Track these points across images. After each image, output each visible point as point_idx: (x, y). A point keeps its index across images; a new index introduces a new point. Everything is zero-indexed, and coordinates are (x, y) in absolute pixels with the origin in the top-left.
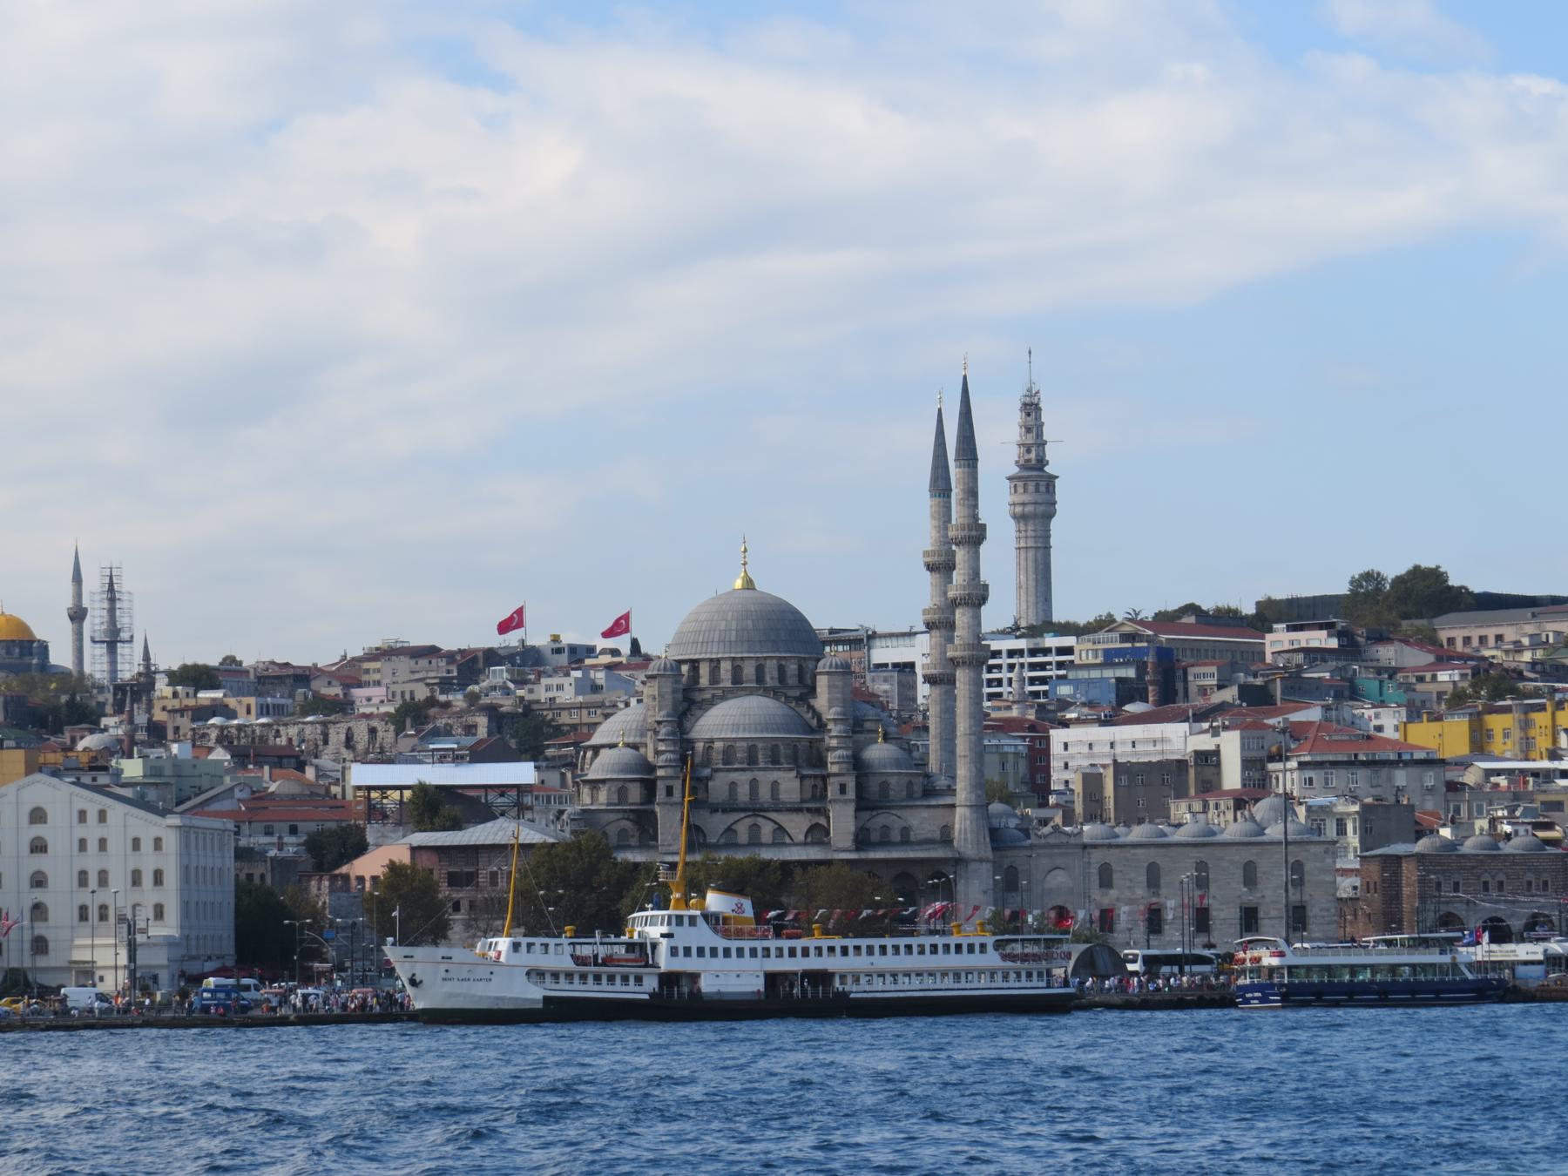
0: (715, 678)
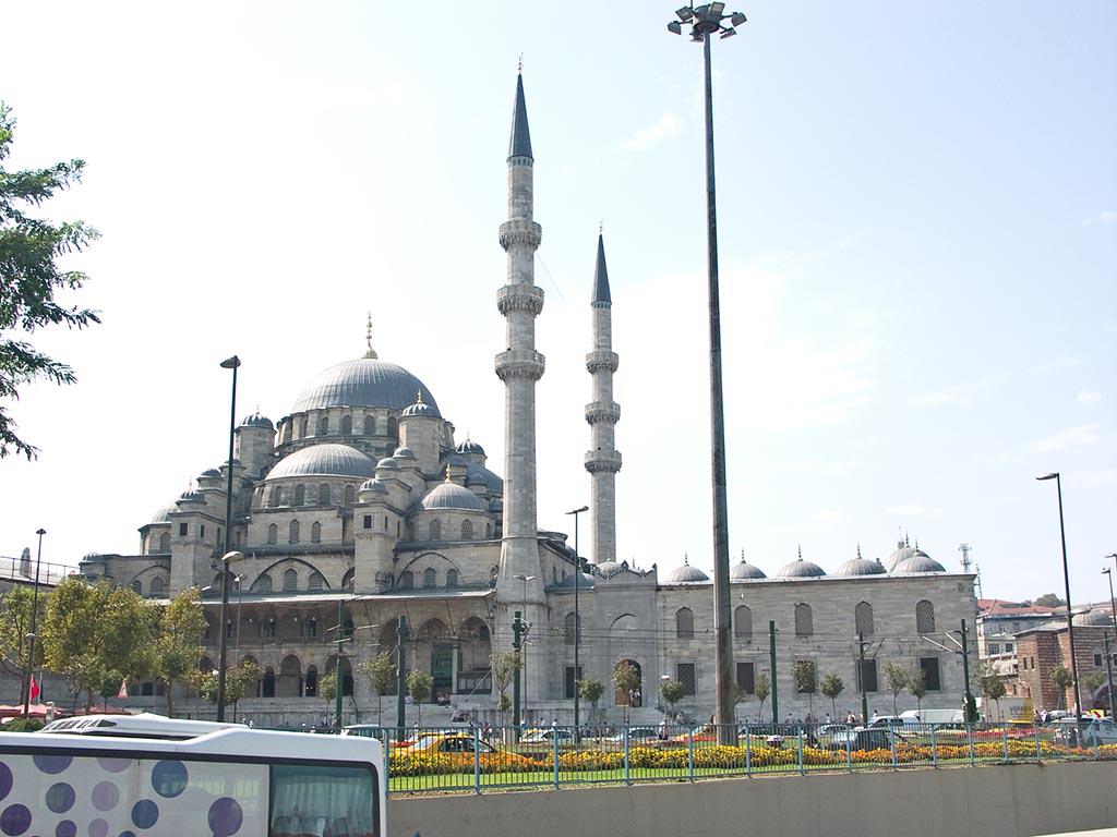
0: (303, 432)
